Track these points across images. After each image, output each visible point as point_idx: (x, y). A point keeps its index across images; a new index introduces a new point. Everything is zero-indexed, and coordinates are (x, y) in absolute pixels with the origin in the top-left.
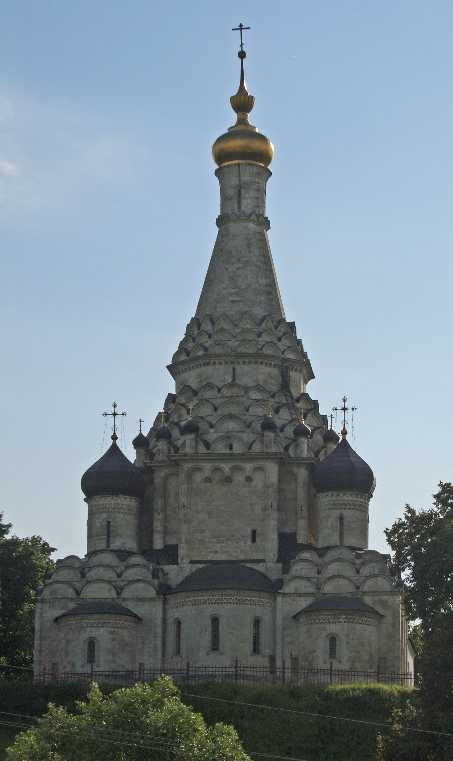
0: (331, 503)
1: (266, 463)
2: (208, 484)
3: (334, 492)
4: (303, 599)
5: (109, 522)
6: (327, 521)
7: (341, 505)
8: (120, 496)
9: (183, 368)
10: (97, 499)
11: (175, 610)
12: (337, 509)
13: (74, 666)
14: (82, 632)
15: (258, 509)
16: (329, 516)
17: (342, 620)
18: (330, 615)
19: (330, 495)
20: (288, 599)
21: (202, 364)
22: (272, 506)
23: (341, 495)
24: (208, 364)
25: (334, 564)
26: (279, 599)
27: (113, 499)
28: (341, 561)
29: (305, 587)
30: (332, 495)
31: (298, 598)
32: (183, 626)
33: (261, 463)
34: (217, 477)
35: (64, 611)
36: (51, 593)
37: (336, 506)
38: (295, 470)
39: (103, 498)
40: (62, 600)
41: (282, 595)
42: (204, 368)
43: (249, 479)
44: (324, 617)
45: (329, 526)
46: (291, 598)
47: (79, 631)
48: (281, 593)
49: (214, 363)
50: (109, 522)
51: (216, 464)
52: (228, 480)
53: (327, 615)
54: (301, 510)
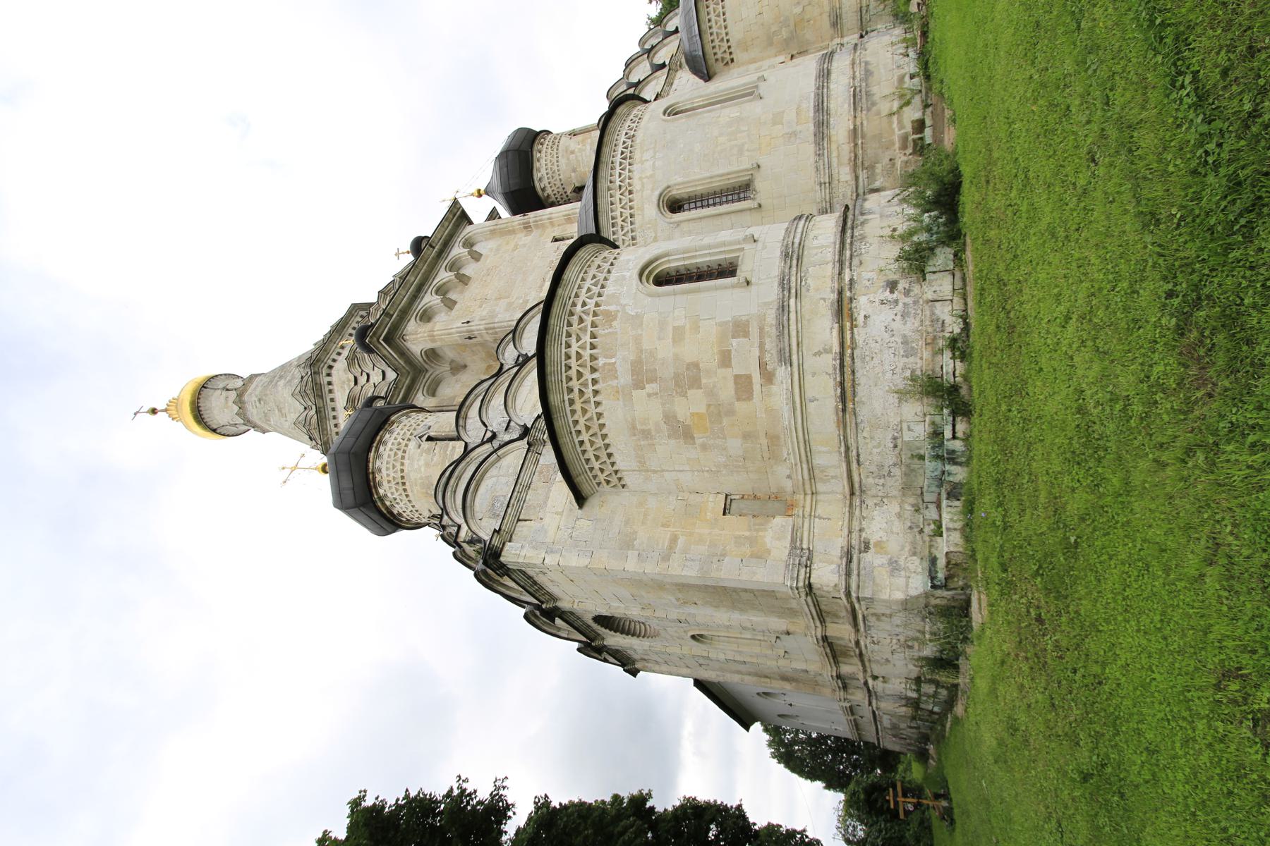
2: (457, 306)
4: (676, 82)
5: (430, 439)
6: (572, 152)
8: (393, 418)
9: (333, 422)
10: (378, 463)
11: (637, 219)
13: (740, 329)
14: (612, 308)
21: (328, 379)
24: (330, 367)
27: (391, 432)
31: (674, 87)
32: (677, 192)
34: (452, 295)
35: (559, 476)
36: (495, 516)
39: (382, 448)
40: (525, 479)
42: (334, 379)
43: (476, 257)
47: (610, 317)
49: (334, 360)
50: (430, 439)
51: (432, 288)
52: (463, 280)
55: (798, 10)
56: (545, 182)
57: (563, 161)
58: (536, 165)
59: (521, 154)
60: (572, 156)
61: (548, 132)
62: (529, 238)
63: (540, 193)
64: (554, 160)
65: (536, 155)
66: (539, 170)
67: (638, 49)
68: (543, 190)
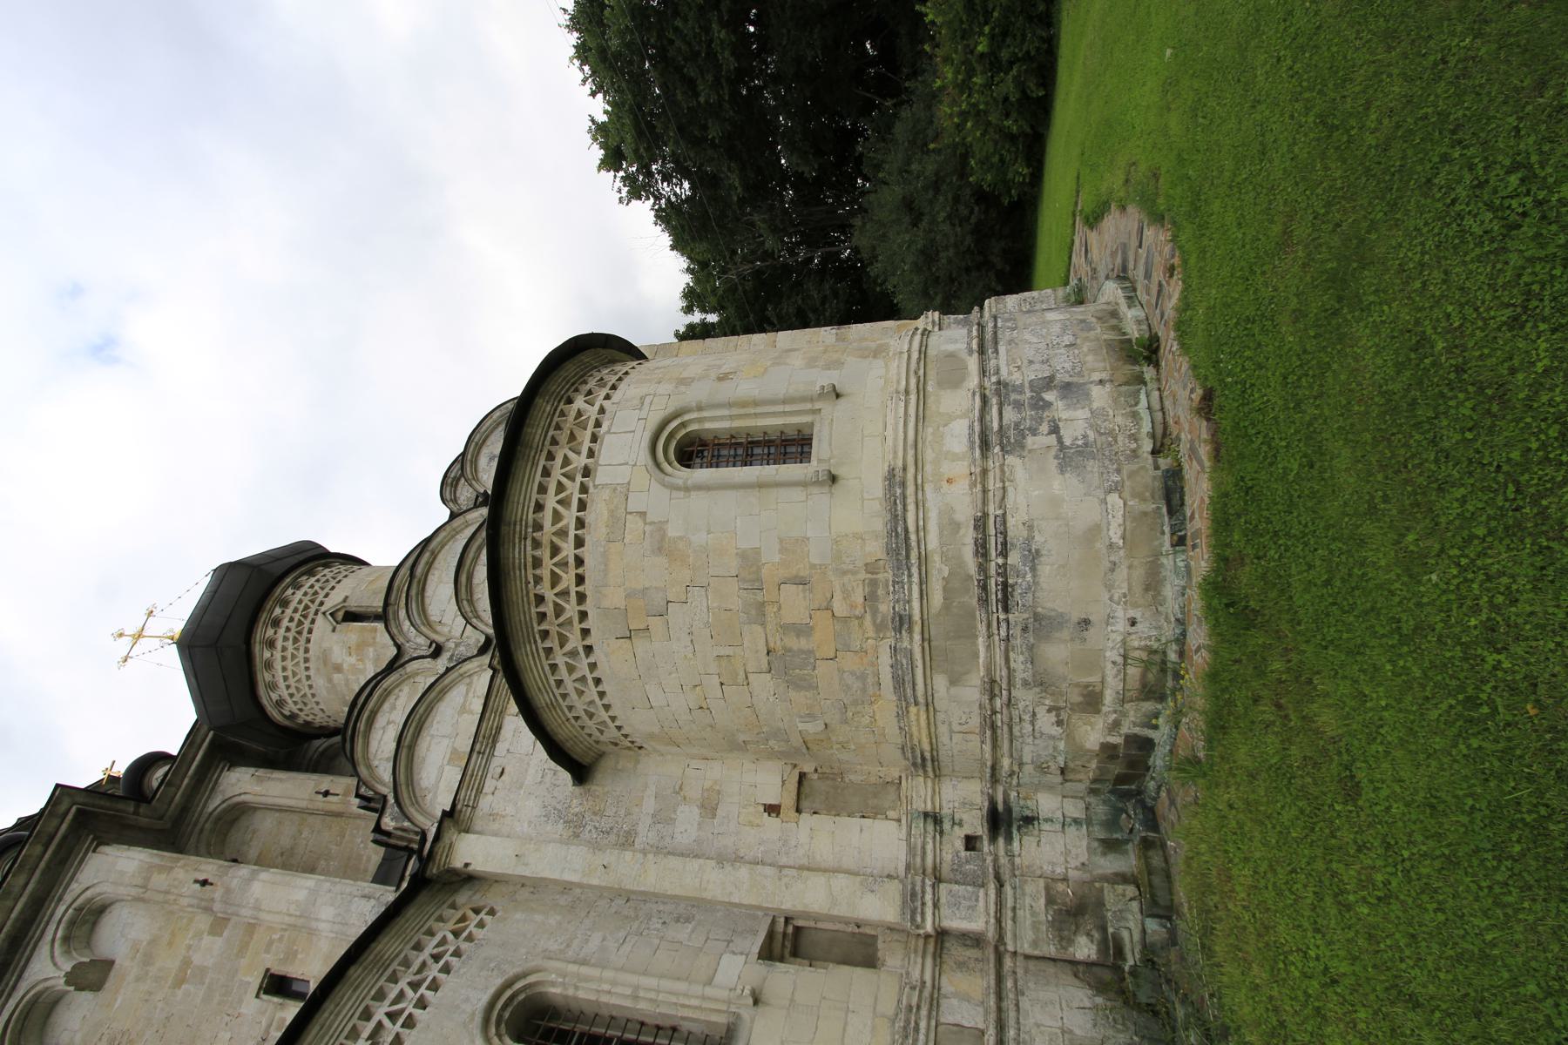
0: (289, 644)
1: (74, 886)
3: (258, 635)
6: (338, 668)
7: (305, 617)
12: (310, 631)
15: (209, 950)
16: (325, 657)
17: (592, 412)
18: (546, 473)
19: (267, 654)
20: (485, 803)
22: (204, 883)
23: (278, 611)
25: (429, 592)
26: (469, 851)
28: (430, 565)
29: (463, 709)
30: (271, 644)
31: (501, 748)
33: (61, 911)
37: (302, 634)
38: (215, 803)
41: (451, 835)
44: (551, 501)
45: (352, 660)
46: (490, 784)
48: (437, 838)
53: (542, 489)
54: (326, 794)
55: (813, 728)
56: (290, 707)
57: (319, 682)
58: (263, 677)
59: (238, 619)
60: (337, 677)
61: (308, 559)
62: (218, 943)
63: (287, 723)
64: (302, 674)
65: (262, 654)
66: (272, 686)
67: (444, 514)
68: (293, 716)
